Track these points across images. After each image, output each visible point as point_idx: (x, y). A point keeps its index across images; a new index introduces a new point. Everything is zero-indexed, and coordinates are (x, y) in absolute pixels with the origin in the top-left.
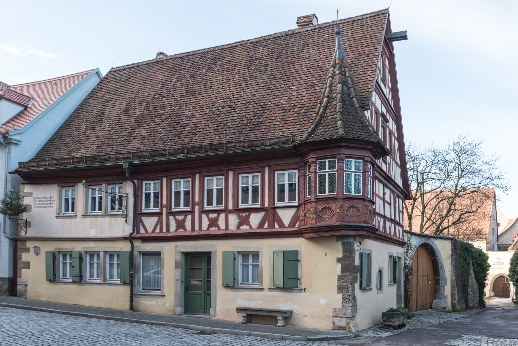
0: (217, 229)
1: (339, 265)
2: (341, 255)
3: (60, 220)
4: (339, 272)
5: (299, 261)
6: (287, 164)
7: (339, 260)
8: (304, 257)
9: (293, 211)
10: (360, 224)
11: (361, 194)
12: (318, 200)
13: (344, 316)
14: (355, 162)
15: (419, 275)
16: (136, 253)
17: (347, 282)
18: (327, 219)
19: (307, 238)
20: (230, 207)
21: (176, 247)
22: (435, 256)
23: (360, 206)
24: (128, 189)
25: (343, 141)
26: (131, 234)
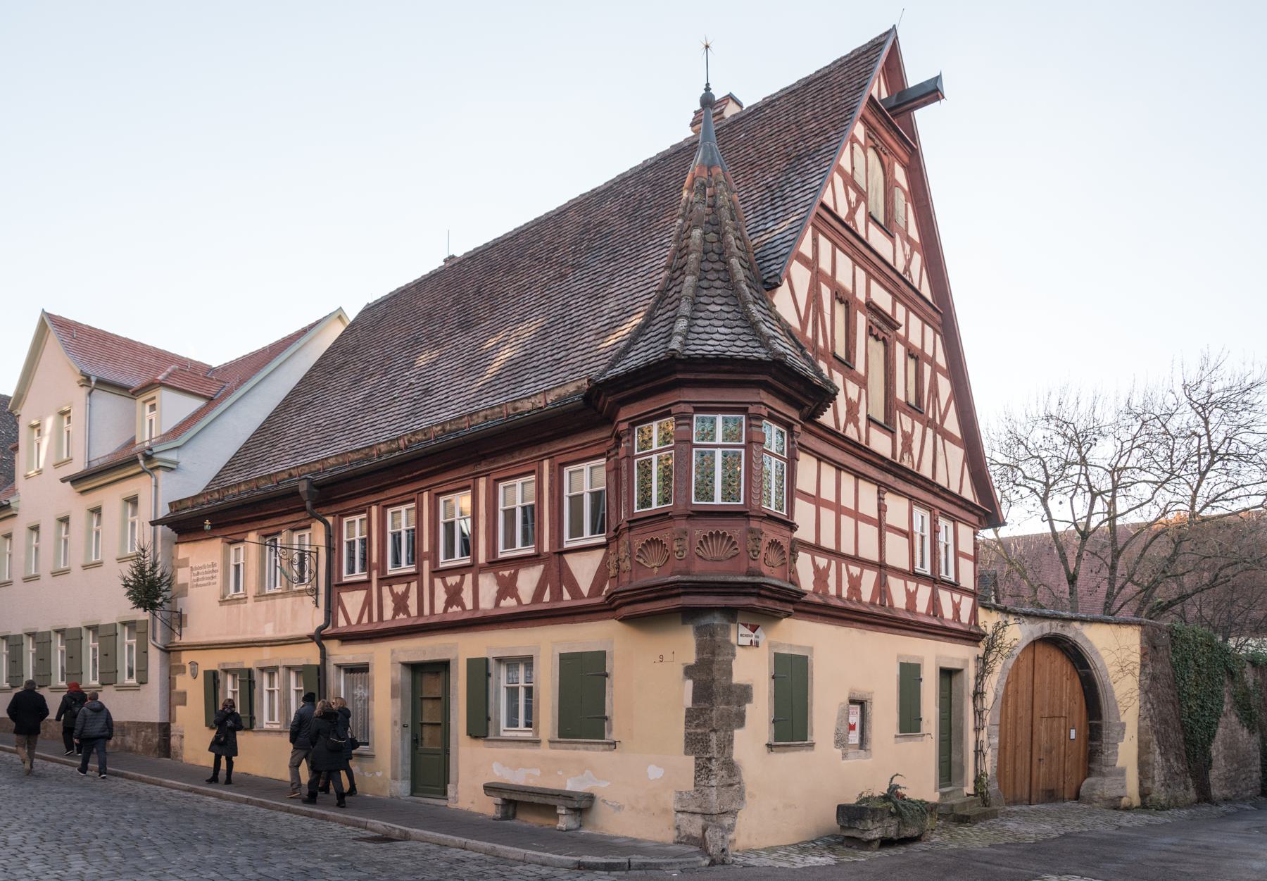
0: (460, 609)
2: (692, 659)
3: (225, 608)
4: (688, 702)
5: (606, 675)
6: (584, 446)
7: (689, 671)
8: (614, 666)
9: (599, 555)
10: (731, 579)
11: (742, 502)
12: (635, 523)
13: (698, 810)
14: (726, 421)
15: (1037, 716)
16: (331, 670)
17: (704, 725)
18: (656, 570)
19: (624, 620)
20: (482, 559)
21: (393, 652)
22: (1088, 667)
24: (316, 536)
25: (680, 367)
26: (321, 629)
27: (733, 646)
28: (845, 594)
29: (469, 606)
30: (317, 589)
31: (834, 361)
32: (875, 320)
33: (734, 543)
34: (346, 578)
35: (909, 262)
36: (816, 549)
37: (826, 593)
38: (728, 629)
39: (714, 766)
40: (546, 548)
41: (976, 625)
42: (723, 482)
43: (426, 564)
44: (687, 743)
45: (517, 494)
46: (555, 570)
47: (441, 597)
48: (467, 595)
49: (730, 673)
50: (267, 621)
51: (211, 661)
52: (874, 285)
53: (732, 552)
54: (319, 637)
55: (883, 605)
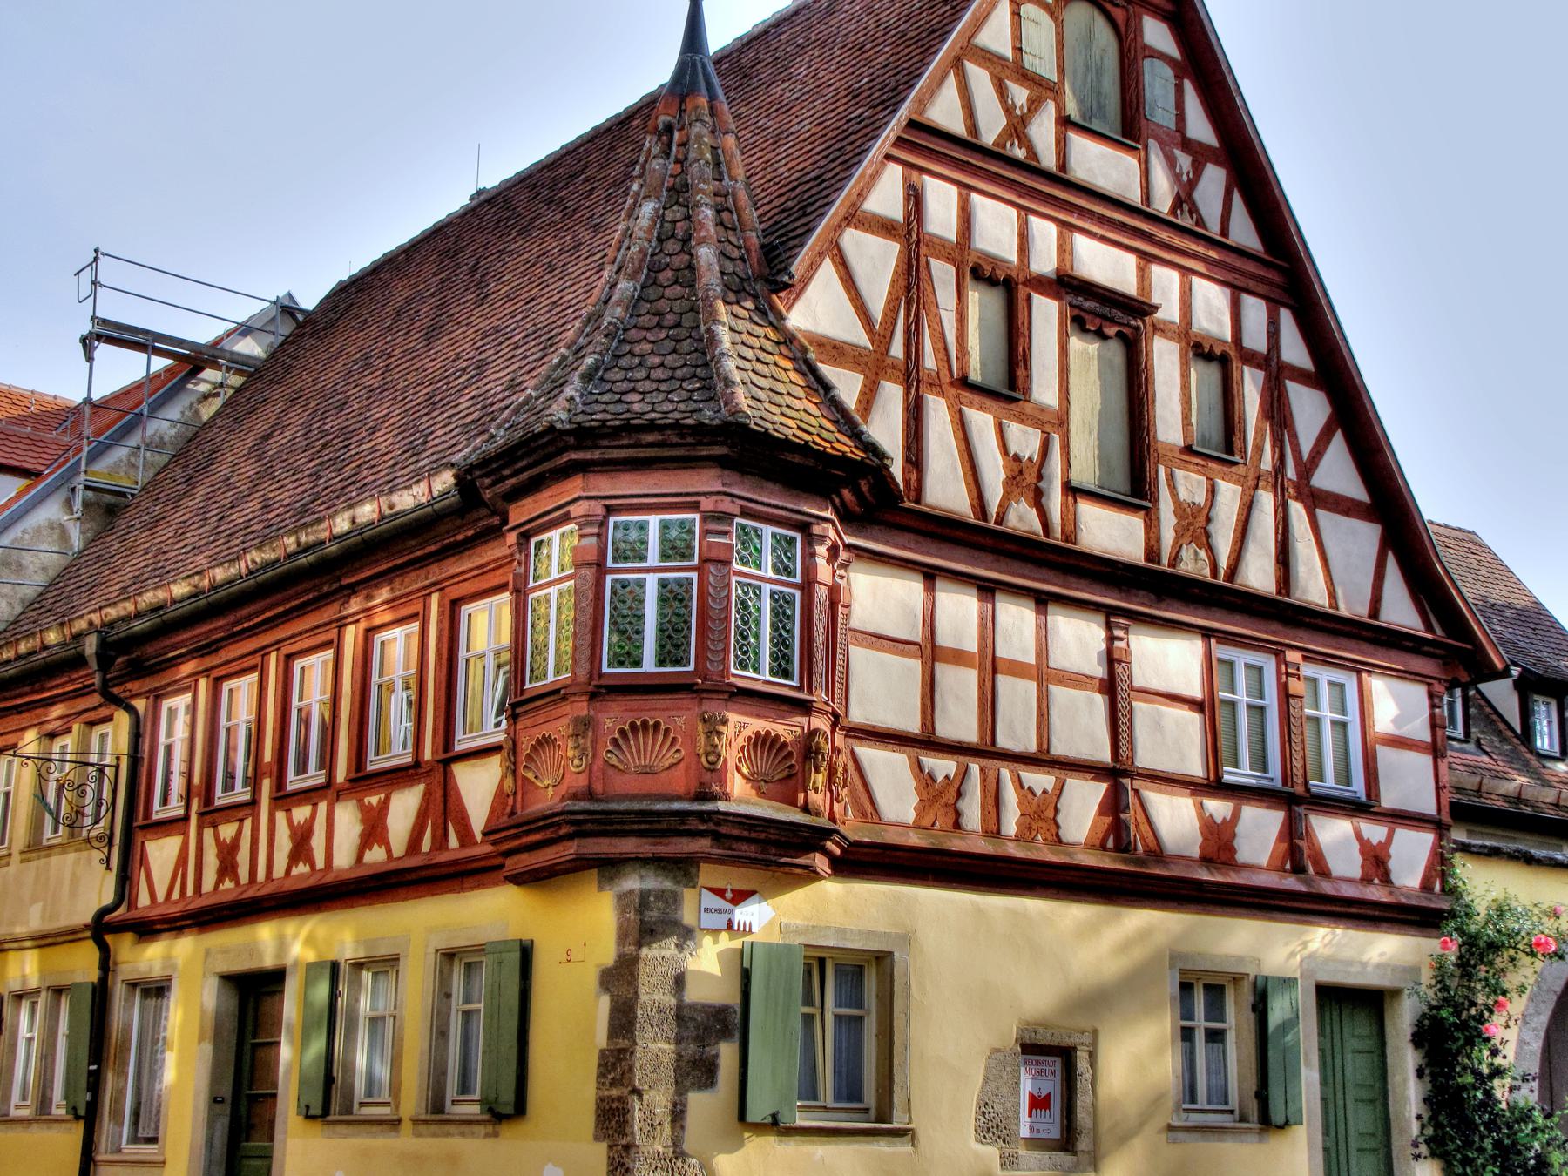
11: (691, 668)
18: (550, 791)
23: (680, 721)
28: (1010, 826)
29: (320, 864)
32: (1088, 304)
34: (159, 813)
35: (1192, 184)
38: (674, 900)
40: (428, 755)
42: (661, 630)
43: (266, 785)
44: (598, 1116)
46: (439, 793)
47: (284, 844)
48: (318, 842)
50: (34, 901)
52: (1082, 243)
54: (102, 928)
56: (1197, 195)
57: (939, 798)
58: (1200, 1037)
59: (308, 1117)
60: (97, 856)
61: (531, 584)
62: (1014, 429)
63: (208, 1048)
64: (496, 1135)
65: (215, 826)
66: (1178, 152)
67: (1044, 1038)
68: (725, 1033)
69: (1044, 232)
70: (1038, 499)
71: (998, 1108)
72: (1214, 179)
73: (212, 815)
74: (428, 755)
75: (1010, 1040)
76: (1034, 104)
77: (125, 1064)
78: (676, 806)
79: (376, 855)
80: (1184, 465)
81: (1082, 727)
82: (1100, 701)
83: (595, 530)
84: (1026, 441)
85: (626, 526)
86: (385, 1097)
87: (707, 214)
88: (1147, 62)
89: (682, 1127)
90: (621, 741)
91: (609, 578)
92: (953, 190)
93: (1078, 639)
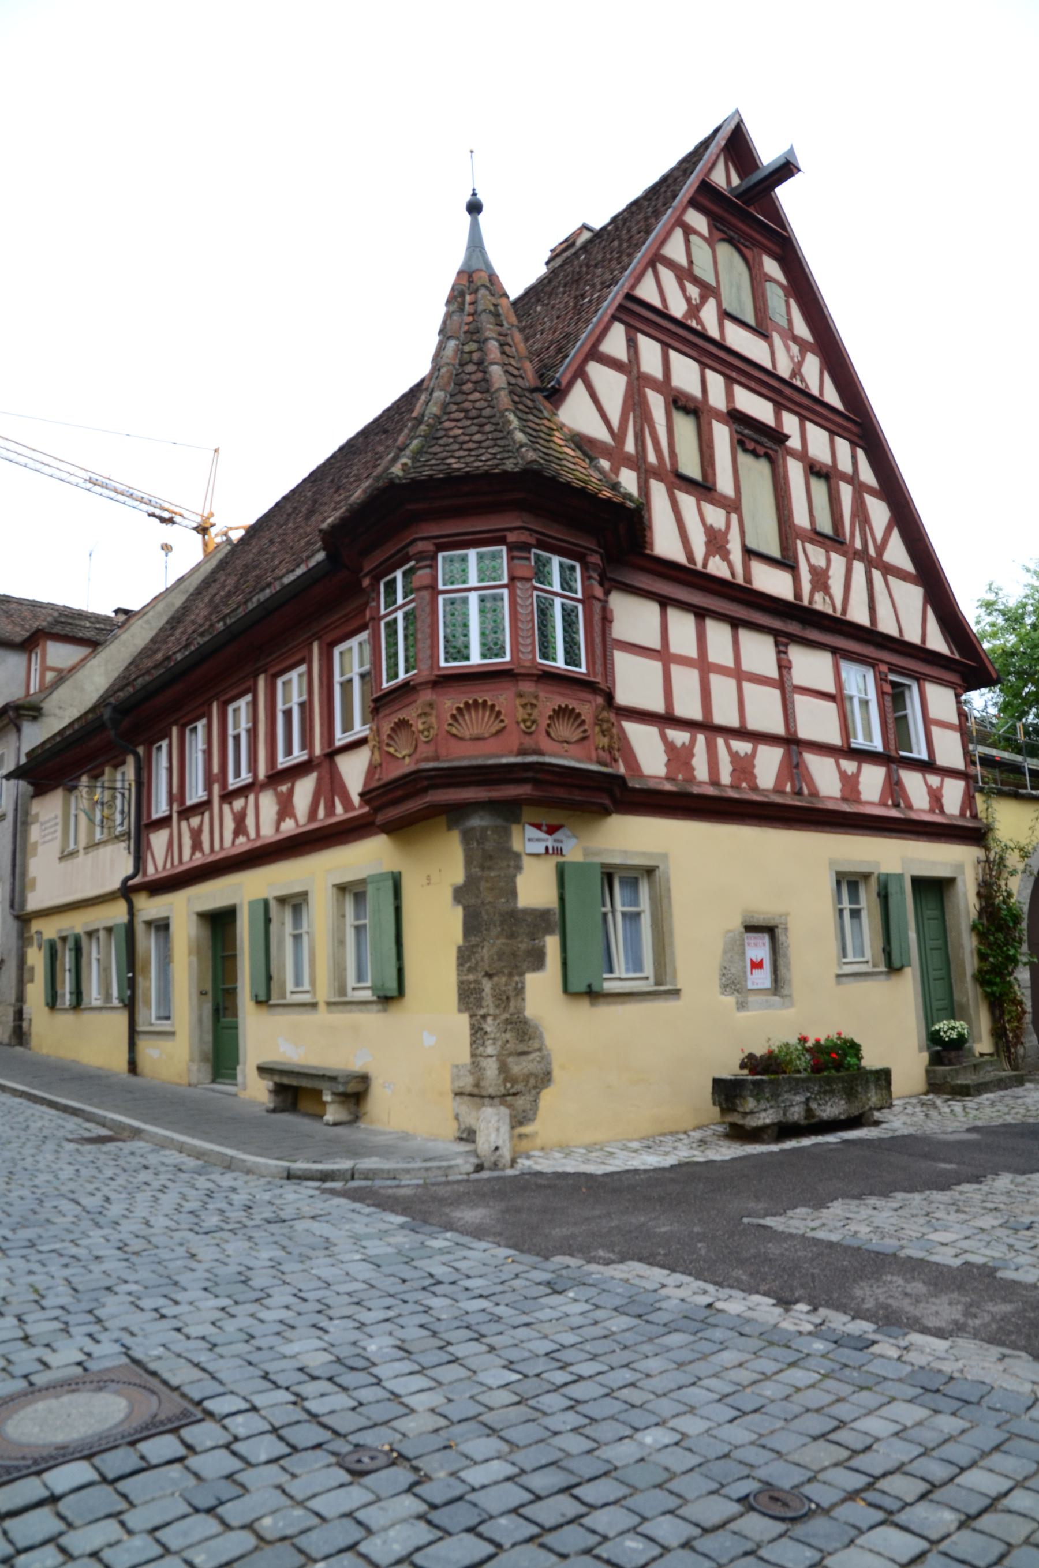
1: (459, 912)
4: (457, 936)
11: (508, 658)
18: (407, 760)
23: (502, 699)
27: (517, 856)
30: (129, 833)
31: (677, 481)
33: (499, 713)
35: (800, 364)
36: (667, 720)
37: (691, 779)
38: (507, 834)
39: (489, 1026)
40: (318, 751)
41: (975, 816)
43: (216, 788)
44: (460, 995)
45: (293, 688)
47: (229, 825)
49: (513, 893)
51: (49, 929)
52: (738, 390)
53: (497, 726)
55: (799, 793)
56: (804, 370)
57: (678, 757)
58: (847, 914)
59: (258, 1002)
60: (123, 845)
61: (383, 612)
62: (708, 509)
63: (194, 959)
64: (385, 1010)
65: (187, 819)
66: (791, 343)
67: (759, 920)
68: (549, 931)
69: (716, 381)
70: (725, 556)
71: (733, 971)
72: (812, 365)
73: (186, 813)
74: (318, 751)
75: (736, 924)
76: (704, 299)
77: (149, 972)
78: (504, 761)
79: (289, 827)
80: (812, 541)
81: (765, 711)
82: (777, 693)
83: (428, 563)
84: (716, 516)
85: (451, 560)
86: (306, 987)
87: (493, 345)
88: (768, 284)
89: (523, 999)
90: (459, 717)
91: (441, 598)
92: (657, 347)
93: (759, 652)
